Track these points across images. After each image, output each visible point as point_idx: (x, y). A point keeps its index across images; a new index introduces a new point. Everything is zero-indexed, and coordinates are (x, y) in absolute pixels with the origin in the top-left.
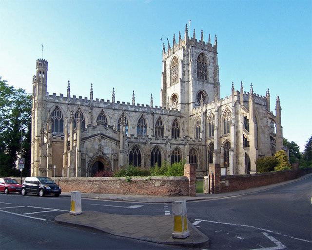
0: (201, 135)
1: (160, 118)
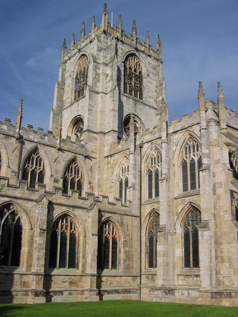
0: (130, 194)
1: (35, 151)
